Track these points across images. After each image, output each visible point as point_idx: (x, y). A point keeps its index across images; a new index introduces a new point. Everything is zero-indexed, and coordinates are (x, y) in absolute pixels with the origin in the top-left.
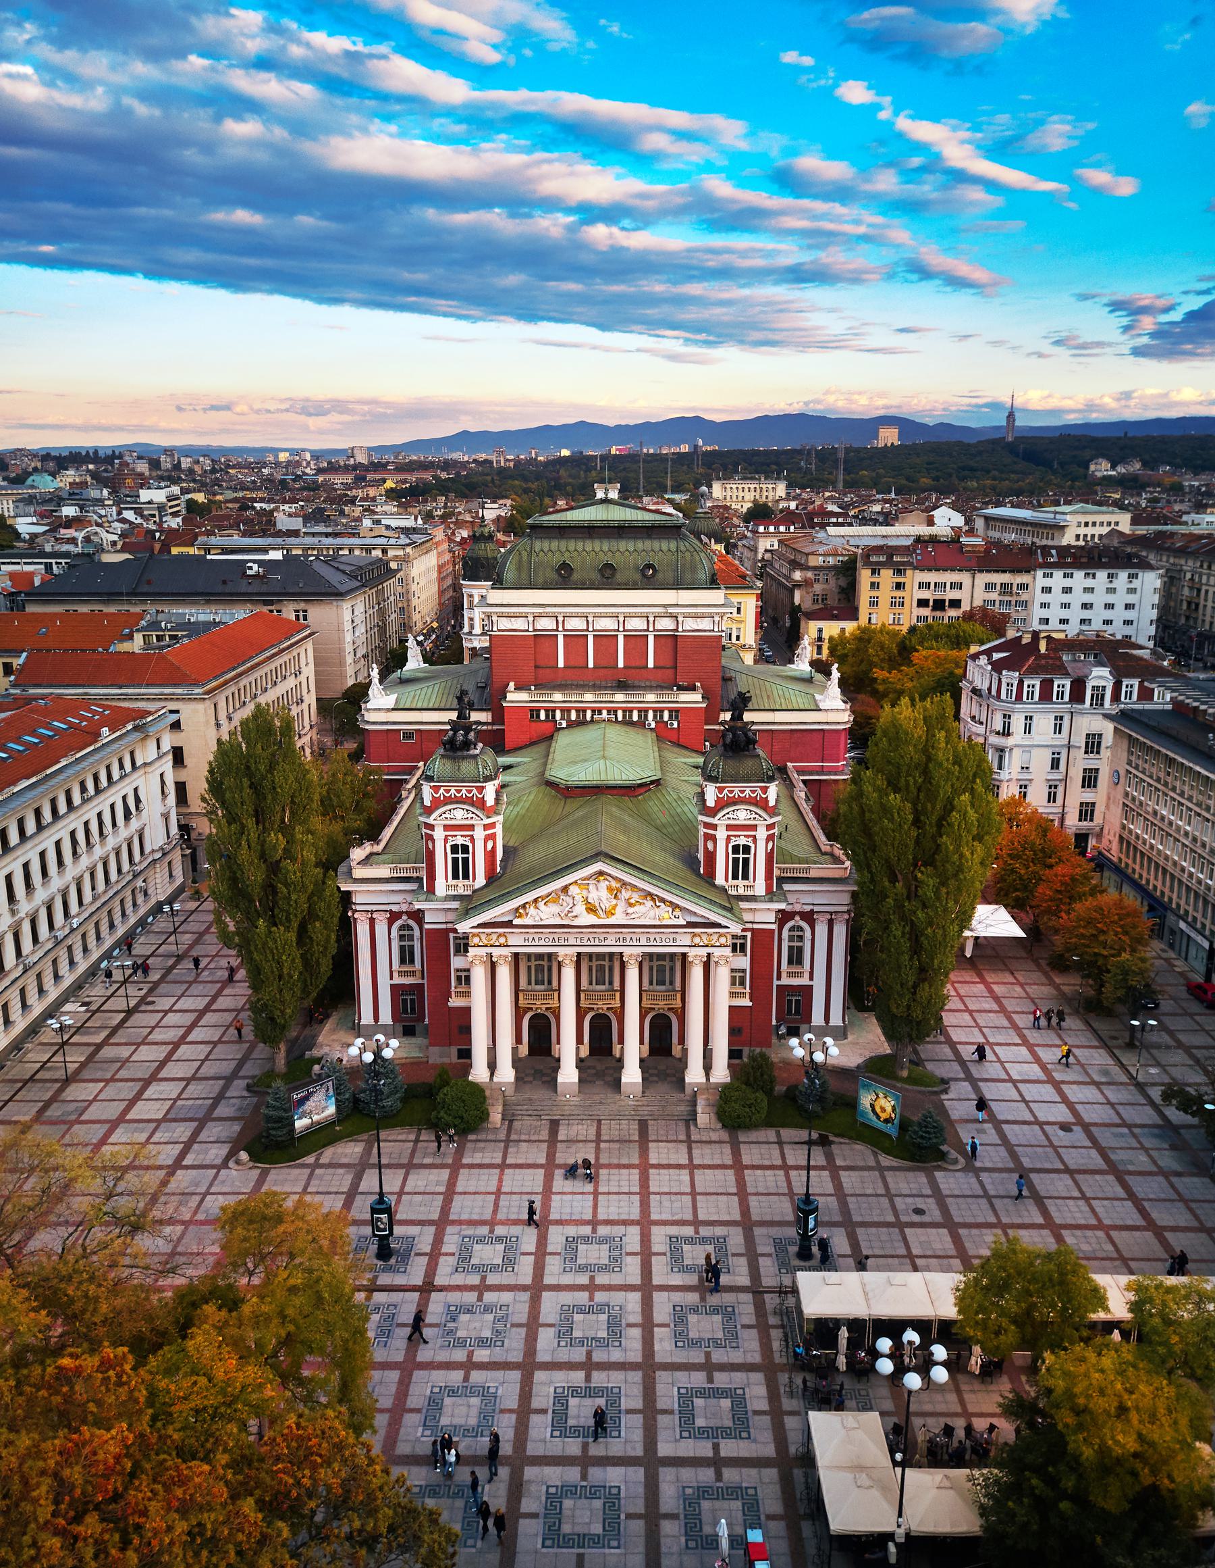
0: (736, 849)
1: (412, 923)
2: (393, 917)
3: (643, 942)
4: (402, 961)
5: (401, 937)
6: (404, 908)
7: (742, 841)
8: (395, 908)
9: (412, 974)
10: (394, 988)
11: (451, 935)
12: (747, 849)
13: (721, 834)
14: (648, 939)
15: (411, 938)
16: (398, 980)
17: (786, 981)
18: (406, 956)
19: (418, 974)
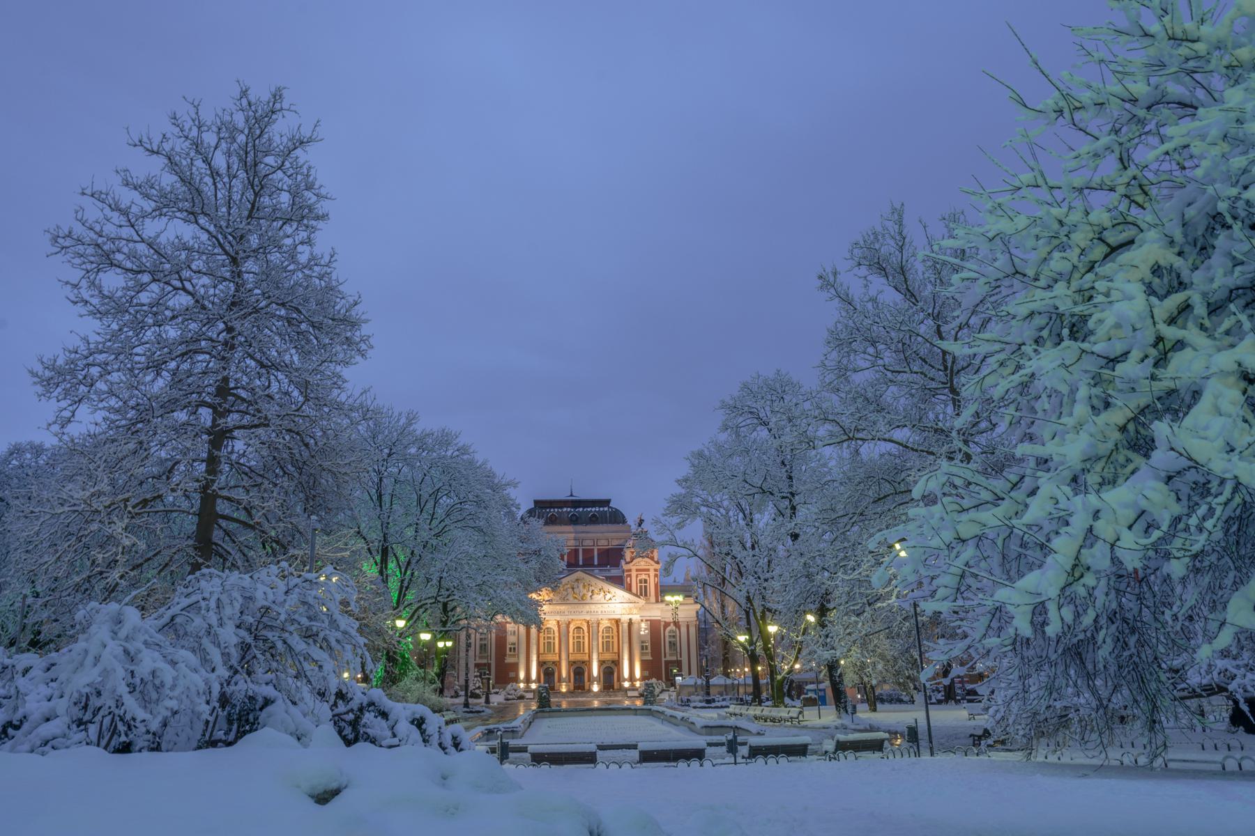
7: (644, 577)
12: (646, 581)
17: (668, 658)
18: (483, 647)
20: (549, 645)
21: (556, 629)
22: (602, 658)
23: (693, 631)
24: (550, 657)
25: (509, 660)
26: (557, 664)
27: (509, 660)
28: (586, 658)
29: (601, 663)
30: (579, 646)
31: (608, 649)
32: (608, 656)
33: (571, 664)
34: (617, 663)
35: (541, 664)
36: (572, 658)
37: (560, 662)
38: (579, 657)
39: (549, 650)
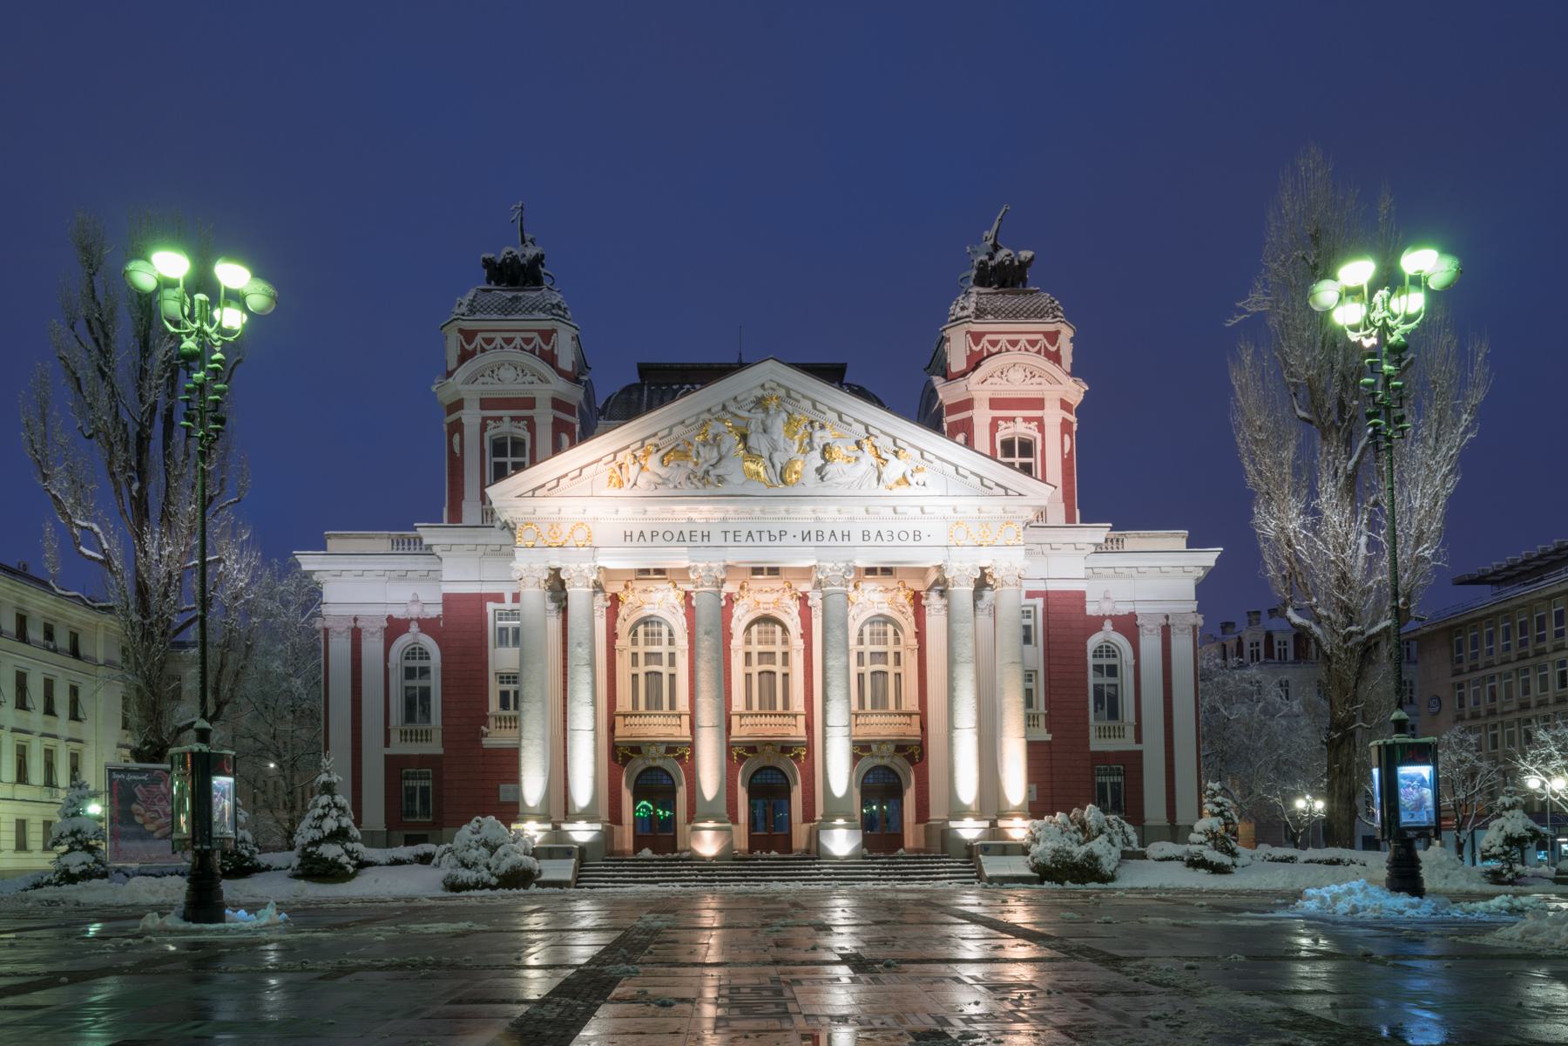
0: (1008, 447)
1: (429, 643)
2: (395, 628)
3: (856, 538)
4: (409, 717)
5: (410, 673)
6: (415, 611)
8: (399, 613)
9: (426, 736)
10: (395, 765)
11: (491, 607)
13: (982, 416)
14: (865, 535)
15: (425, 672)
16: (399, 748)
18: (416, 704)
19: (437, 736)
20: (655, 690)
21: (679, 623)
22: (863, 733)
23: (1183, 646)
24: (657, 728)
25: (495, 738)
26: (683, 752)
27: (495, 738)
28: (798, 732)
29: (861, 749)
30: (769, 687)
31: (879, 701)
32: (882, 727)
33: (737, 753)
34: (913, 752)
35: (621, 754)
36: (740, 731)
37: (692, 746)
38: (767, 728)
39: (654, 702)
